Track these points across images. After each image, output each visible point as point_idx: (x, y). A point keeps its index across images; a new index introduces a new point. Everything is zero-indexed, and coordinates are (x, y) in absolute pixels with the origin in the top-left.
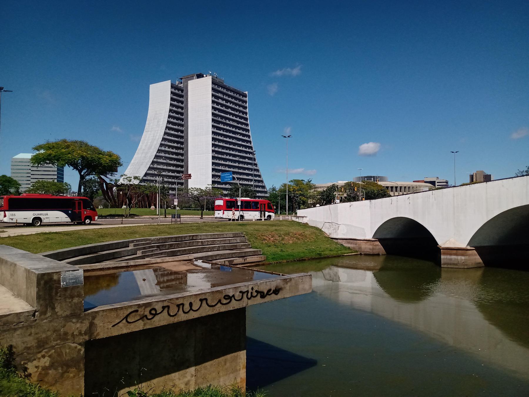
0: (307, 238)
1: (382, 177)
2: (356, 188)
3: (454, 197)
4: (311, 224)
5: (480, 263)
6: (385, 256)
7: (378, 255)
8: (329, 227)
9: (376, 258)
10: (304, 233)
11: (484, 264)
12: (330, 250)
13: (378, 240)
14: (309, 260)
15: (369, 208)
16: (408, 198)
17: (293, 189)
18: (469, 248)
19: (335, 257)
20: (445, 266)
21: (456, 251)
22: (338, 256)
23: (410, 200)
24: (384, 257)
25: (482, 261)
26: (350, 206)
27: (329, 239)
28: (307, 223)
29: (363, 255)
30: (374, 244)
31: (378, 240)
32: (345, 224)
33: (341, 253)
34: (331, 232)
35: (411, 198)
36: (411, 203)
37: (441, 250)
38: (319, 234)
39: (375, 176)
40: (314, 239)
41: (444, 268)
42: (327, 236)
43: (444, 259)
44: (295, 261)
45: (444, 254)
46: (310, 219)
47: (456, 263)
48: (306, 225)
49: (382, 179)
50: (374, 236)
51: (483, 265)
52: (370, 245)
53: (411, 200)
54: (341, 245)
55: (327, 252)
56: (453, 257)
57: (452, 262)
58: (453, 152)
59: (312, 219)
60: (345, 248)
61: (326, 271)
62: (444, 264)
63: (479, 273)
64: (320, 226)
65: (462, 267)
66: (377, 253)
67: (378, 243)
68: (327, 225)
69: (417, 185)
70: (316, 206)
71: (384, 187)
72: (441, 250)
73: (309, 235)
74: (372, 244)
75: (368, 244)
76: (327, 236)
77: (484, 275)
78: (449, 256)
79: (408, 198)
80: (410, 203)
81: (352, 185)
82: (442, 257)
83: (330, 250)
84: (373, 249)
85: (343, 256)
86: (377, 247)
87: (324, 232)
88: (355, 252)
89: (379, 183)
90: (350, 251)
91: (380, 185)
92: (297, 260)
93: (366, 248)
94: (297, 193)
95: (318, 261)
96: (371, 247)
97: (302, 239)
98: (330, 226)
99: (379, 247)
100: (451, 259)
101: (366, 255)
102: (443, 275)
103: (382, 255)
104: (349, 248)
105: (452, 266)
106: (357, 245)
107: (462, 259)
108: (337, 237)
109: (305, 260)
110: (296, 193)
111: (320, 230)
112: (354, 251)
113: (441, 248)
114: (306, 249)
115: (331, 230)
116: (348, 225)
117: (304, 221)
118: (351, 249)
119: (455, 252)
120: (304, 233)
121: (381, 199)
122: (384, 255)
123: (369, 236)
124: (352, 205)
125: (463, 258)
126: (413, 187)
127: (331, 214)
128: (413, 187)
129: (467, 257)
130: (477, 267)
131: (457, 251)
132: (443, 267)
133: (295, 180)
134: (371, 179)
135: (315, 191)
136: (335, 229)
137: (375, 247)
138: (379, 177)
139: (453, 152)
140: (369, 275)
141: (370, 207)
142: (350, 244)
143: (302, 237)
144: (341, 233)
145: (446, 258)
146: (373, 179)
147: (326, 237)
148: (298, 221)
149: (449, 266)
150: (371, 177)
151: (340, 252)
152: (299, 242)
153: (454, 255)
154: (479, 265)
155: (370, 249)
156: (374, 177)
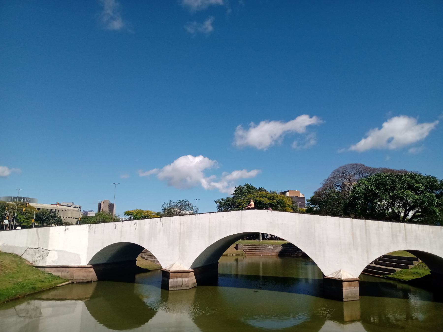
0: (7, 268)
1: (34, 199)
2: (24, 208)
3: (181, 225)
6: (97, 282)
7: (91, 282)
8: (34, 254)
9: (89, 285)
12: (42, 282)
13: (92, 266)
14: (23, 297)
15: (87, 232)
16: (135, 224)
20: (172, 289)
21: (181, 273)
23: (136, 225)
24: (96, 283)
26: (66, 230)
27: (33, 267)
29: (75, 283)
30: (88, 271)
31: (92, 266)
32: (57, 250)
33: (54, 284)
34: (35, 259)
35: (137, 224)
36: (137, 229)
37: (170, 274)
38: (20, 263)
39: (25, 198)
40: (16, 269)
41: (171, 290)
42: (30, 265)
43: (172, 282)
44: (7, 301)
45: (173, 277)
46: (4, 244)
47: (181, 285)
49: (32, 200)
52: (85, 272)
53: (137, 225)
54: (49, 274)
56: (179, 279)
57: (178, 284)
58: (114, 184)
59: (7, 244)
62: (172, 287)
64: (19, 253)
65: (185, 288)
66: (90, 280)
67: (92, 270)
68: (31, 251)
69: (66, 209)
70: (16, 229)
71: (35, 208)
72: (170, 274)
73: (10, 264)
76: (29, 264)
77: (197, 292)
78: (176, 279)
79: (135, 224)
80: (136, 229)
81: (27, 206)
82: (171, 280)
85: (57, 287)
87: (25, 259)
88: (66, 281)
89: (31, 204)
91: (32, 207)
92: (10, 300)
93: (80, 276)
96: (85, 274)
98: (35, 252)
99: (92, 274)
100: (177, 282)
103: (95, 281)
104: (59, 277)
105: (178, 288)
106: (69, 273)
107: (186, 281)
108: (44, 265)
109: (18, 298)
111: (20, 257)
112: (65, 279)
113: (170, 272)
115: (36, 258)
116: (61, 251)
118: (61, 278)
119: (180, 274)
121: (104, 223)
122: (96, 281)
123: (85, 262)
124: (68, 229)
125: (186, 279)
126: (62, 210)
127: (39, 238)
128: (62, 210)
132: (170, 290)
134: (21, 200)
136: (42, 256)
137: (89, 274)
139: (114, 184)
140: (80, 306)
141: (89, 231)
142: (60, 272)
145: (173, 282)
146: (24, 200)
147: (29, 266)
149: (175, 289)
150: (21, 198)
151: (53, 283)
153: (180, 278)
155: (84, 277)
156: (24, 198)
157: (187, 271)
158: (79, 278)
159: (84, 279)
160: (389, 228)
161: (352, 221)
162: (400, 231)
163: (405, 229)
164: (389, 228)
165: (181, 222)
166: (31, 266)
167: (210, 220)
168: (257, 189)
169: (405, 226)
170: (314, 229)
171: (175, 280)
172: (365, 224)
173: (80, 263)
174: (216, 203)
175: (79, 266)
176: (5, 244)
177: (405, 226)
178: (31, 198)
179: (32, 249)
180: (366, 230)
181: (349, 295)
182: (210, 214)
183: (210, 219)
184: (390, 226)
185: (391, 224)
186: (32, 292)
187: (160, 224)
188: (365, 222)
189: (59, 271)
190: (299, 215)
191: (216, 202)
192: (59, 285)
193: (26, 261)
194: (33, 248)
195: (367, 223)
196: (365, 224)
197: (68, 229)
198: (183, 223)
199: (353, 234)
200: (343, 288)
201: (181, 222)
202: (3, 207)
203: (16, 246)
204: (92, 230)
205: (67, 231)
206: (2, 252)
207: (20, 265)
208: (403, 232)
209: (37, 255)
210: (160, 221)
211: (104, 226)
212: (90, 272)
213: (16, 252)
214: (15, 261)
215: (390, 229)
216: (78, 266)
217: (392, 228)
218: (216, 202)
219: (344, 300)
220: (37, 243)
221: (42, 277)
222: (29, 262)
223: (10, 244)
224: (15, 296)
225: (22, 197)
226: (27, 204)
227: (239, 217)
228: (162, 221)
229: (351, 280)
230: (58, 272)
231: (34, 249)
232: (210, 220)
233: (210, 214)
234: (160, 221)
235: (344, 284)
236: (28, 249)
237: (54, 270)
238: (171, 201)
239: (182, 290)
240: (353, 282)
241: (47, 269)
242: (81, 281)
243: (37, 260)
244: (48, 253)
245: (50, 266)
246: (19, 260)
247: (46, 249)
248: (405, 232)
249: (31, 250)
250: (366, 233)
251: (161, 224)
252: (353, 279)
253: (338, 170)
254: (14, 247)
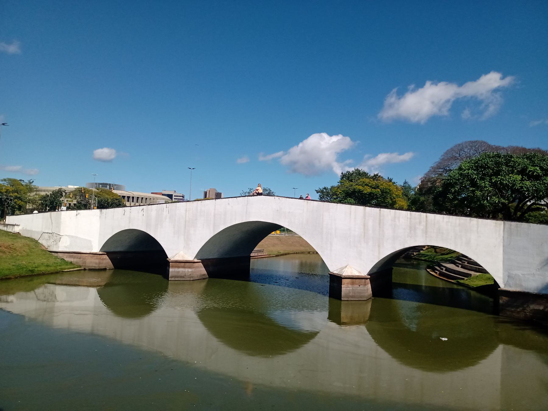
0: (16, 251)
1: (120, 185)
2: (87, 194)
3: (186, 212)
4: (24, 234)
5: (204, 275)
6: (113, 270)
7: (105, 269)
8: (49, 238)
9: (102, 273)
10: (13, 244)
11: (208, 276)
12: (47, 266)
13: (106, 253)
15: (98, 218)
16: (142, 210)
17: (6, 190)
18: (196, 260)
19: (52, 273)
20: (173, 279)
21: (184, 263)
22: (57, 273)
23: (144, 211)
24: (112, 271)
25: (206, 273)
26: (77, 215)
27: (47, 252)
28: (18, 233)
29: (87, 270)
30: (101, 258)
31: (106, 253)
32: (69, 236)
33: (60, 269)
34: (50, 244)
35: (144, 210)
38: (34, 247)
39: (111, 184)
41: (171, 280)
42: (45, 249)
45: (173, 267)
46: (23, 228)
48: (17, 235)
49: (118, 187)
50: (101, 250)
51: (207, 276)
52: (97, 259)
53: (144, 212)
54: (62, 259)
55: (43, 269)
56: (181, 270)
57: (179, 274)
58: (190, 169)
59: (26, 228)
60: (67, 263)
61: (40, 291)
62: (172, 277)
63: (203, 284)
65: (188, 279)
66: (104, 268)
67: (106, 257)
68: (46, 236)
70: (33, 213)
71: (120, 196)
73: (21, 248)
74: (98, 257)
75: (94, 258)
77: (207, 286)
78: (177, 269)
79: (142, 210)
80: (143, 215)
81: (83, 192)
82: (171, 270)
83: (47, 266)
84: (100, 263)
85: (63, 272)
86: (104, 261)
87: (41, 244)
88: (77, 267)
89: (115, 191)
90: (73, 267)
91: (116, 194)
93: (92, 263)
94: (12, 195)
95: (29, 279)
96: (97, 261)
97: (9, 252)
98: (49, 237)
99: (107, 262)
100: (179, 272)
101: (90, 270)
102: (170, 287)
104: (71, 263)
105: (179, 279)
106: (81, 259)
107: (189, 272)
109: (10, 279)
110: (10, 195)
111: (37, 242)
113: (170, 261)
114: (13, 265)
115: (51, 242)
116: (72, 237)
117: (16, 229)
118: (74, 264)
120: (13, 244)
123: (96, 248)
124: (79, 213)
125: (190, 270)
126: (150, 199)
127: (52, 223)
128: (150, 199)
129: (193, 270)
130: (202, 279)
131: (184, 264)
133: (10, 180)
134: (107, 187)
135: (36, 194)
137: (101, 261)
138: (115, 185)
139: (190, 169)
140: (93, 292)
141: (100, 217)
143: (9, 251)
144: (63, 246)
145: (174, 271)
146: (109, 186)
147: (43, 250)
148: (6, 230)
149: (177, 279)
150: (107, 184)
151: (59, 268)
152: (4, 256)
154: (204, 277)
155: (96, 263)
156: (110, 185)
157: (190, 262)
158: (91, 265)
159: (97, 266)
160: (408, 218)
161: (365, 210)
162: (420, 223)
163: (426, 220)
164: (408, 218)
165: (186, 209)
166: (45, 250)
167: (215, 207)
168: (370, 175)
169: (426, 216)
170: (323, 218)
171: (177, 270)
172: (380, 213)
173: (92, 250)
174: (318, 193)
175: (91, 253)
176: (25, 228)
177: (426, 216)
178: (119, 185)
179: (46, 234)
180: (380, 221)
181: (351, 294)
182: (216, 200)
183: (215, 206)
184: (409, 216)
185: (410, 214)
186: (30, 273)
187: (166, 211)
188: (380, 210)
189: (71, 257)
190: (308, 202)
191: (317, 191)
192: (65, 270)
193: (42, 246)
195: (382, 212)
196: (380, 213)
197: (79, 213)
198: (189, 210)
199: (365, 225)
200: (343, 286)
201: (186, 209)
202: (60, 192)
203: (34, 230)
204: (103, 216)
205: (78, 216)
206: (22, 236)
207: (33, 249)
208: (424, 223)
209: (52, 240)
210: (166, 208)
212: (103, 259)
213: (34, 237)
214: (28, 245)
215: (409, 220)
216: (89, 253)
217: (410, 219)
218: (317, 191)
219: (342, 299)
221: (52, 261)
222: (44, 247)
223: (28, 228)
224: (7, 276)
225: (108, 184)
226: (83, 190)
227: (245, 204)
228: (168, 207)
229: (355, 277)
230: (70, 258)
232: (215, 207)
233: (216, 200)
234: (166, 208)
235: (344, 281)
237: (67, 256)
238: (251, 189)
239: (185, 280)
240: (358, 280)
241: (60, 255)
242: (93, 268)
243: (51, 245)
244: (61, 238)
245: (62, 252)
246: (35, 244)
248: (426, 224)
249: (46, 235)
250: (380, 224)
252: (358, 276)
253: (452, 149)
254: (31, 231)
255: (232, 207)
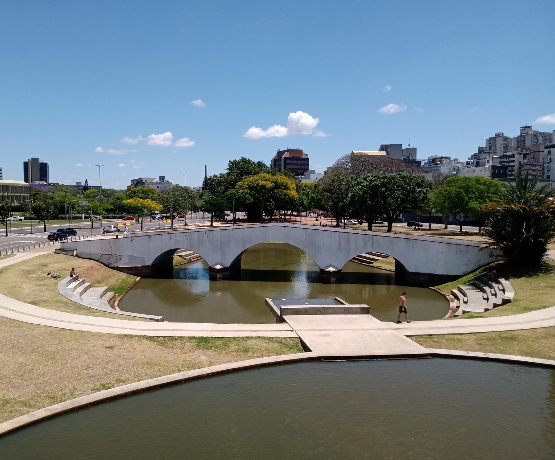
8: (109, 258)
26: (132, 240)
34: (111, 262)
35: (188, 235)
80: (187, 239)
98: (109, 257)
162: (369, 240)
163: (372, 239)
172: (348, 236)
179: (106, 255)
194: (107, 254)
195: (349, 235)
196: (348, 236)
197: (133, 239)
199: (340, 243)
204: (152, 240)
208: (371, 241)
211: (162, 237)
217: (364, 238)
220: (110, 250)
231: (108, 255)
236: (104, 255)
243: (112, 263)
244: (121, 258)
247: (118, 255)
248: (373, 241)
251: (207, 236)
255: (255, 233)
